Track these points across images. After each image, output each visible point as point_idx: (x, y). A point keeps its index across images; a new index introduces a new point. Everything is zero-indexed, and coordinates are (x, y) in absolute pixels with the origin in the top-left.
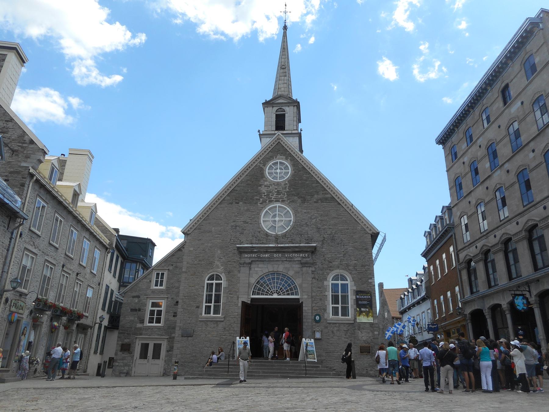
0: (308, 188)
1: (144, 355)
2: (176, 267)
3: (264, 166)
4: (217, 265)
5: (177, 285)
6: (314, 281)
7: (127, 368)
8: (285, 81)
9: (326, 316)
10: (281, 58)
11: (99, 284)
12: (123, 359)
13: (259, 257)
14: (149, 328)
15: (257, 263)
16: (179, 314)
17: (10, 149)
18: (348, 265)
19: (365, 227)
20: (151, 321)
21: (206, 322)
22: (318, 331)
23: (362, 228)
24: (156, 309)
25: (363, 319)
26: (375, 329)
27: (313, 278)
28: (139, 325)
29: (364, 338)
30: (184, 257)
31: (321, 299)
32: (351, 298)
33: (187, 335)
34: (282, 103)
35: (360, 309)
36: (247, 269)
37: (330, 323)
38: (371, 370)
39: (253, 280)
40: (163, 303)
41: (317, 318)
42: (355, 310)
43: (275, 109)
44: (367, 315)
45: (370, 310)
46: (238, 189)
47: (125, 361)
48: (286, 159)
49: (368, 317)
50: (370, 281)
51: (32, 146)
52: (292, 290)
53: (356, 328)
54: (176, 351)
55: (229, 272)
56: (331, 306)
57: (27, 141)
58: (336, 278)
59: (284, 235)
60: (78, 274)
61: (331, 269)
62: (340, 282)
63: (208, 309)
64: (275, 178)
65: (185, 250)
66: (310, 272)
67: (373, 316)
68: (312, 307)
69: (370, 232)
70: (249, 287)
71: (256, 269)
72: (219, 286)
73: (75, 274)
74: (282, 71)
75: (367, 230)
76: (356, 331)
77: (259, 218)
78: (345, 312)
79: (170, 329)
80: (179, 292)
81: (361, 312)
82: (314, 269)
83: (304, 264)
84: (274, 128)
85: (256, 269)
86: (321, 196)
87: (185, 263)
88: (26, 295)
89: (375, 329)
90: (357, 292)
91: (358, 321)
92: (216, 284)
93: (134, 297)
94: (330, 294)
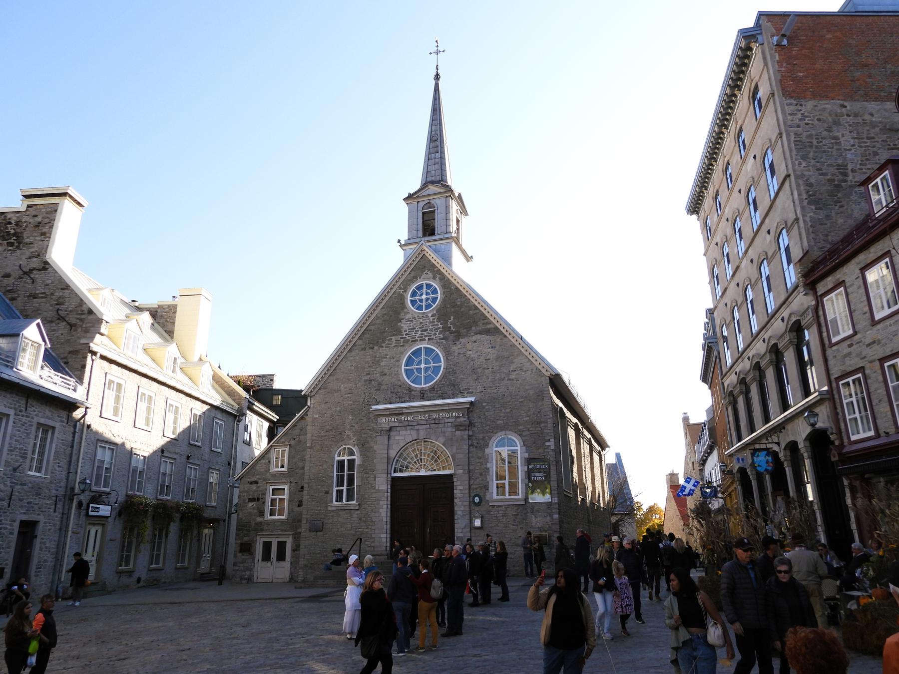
0: (464, 316)
1: (266, 557)
2: (300, 441)
3: (405, 291)
5: (300, 465)
7: (248, 573)
8: (437, 160)
9: (488, 497)
10: (431, 125)
11: (229, 464)
12: (243, 562)
13: (400, 422)
15: (398, 429)
16: (305, 502)
17: (69, 324)
19: (540, 367)
21: (338, 510)
22: (477, 517)
23: (537, 368)
24: (278, 497)
25: (538, 497)
27: (469, 446)
28: (259, 519)
29: (539, 525)
30: (308, 428)
31: (481, 474)
33: (317, 528)
34: (430, 195)
36: (386, 438)
37: (493, 506)
38: (548, 568)
39: (393, 453)
40: (286, 487)
41: (477, 500)
42: (527, 486)
43: (421, 204)
46: (372, 328)
47: (246, 565)
48: (434, 278)
50: (547, 444)
51: (91, 317)
54: (303, 551)
56: (495, 482)
57: (86, 312)
59: (432, 389)
60: (188, 458)
63: (339, 493)
64: (420, 308)
66: (466, 437)
68: (470, 486)
69: (547, 374)
70: (388, 463)
71: (397, 438)
72: (352, 462)
73: (185, 457)
74: (433, 144)
75: (544, 371)
77: (399, 366)
78: (513, 489)
79: (294, 522)
80: (303, 474)
82: (471, 433)
83: (458, 427)
84: (420, 234)
85: (397, 438)
86: (481, 327)
87: (309, 435)
88: (109, 494)
90: (529, 461)
91: (530, 501)
92: (348, 460)
93: (251, 483)
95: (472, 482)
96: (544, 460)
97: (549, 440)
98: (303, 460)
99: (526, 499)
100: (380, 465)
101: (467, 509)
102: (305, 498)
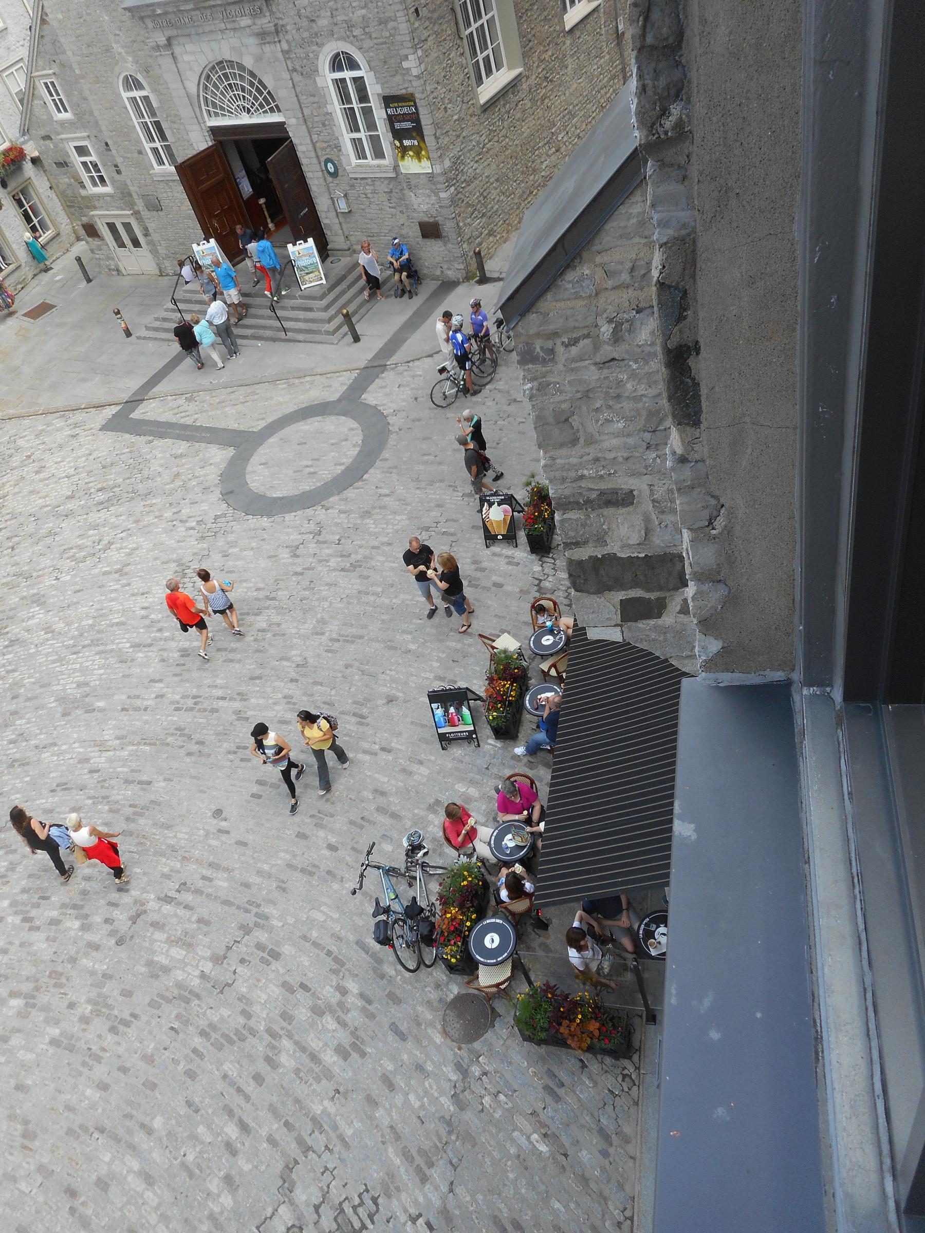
2: (63, 65)
4: (120, 54)
6: (297, 78)
14: (99, 197)
15: (181, 40)
16: (122, 168)
18: (350, 26)
20: (95, 184)
25: (411, 166)
26: (439, 186)
28: (83, 192)
29: (424, 208)
31: (324, 125)
32: (380, 115)
35: (401, 143)
36: (171, 60)
37: (356, 179)
38: (449, 269)
39: (192, 88)
41: (330, 165)
42: (392, 144)
44: (418, 156)
45: (422, 145)
49: (420, 160)
50: (405, 65)
52: (270, 102)
53: (405, 185)
54: (155, 237)
55: (148, 72)
58: (337, 63)
61: (317, 39)
62: (347, 74)
65: (55, 17)
66: (280, 55)
67: (429, 158)
68: (314, 144)
76: (405, 192)
80: (97, 122)
81: (404, 150)
82: (285, 46)
83: (262, 35)
85: (187, 58)
87: (69, 53)
89: (439, 186)
91: (403, 171)
94: (336, 107)
95: (315, 137)
96: (408, 99)
97: (406, 58)
98: (85, 99)
99: (396, 168)
100: (186, 112)
101: (322, 180)
102: (119, 161)
